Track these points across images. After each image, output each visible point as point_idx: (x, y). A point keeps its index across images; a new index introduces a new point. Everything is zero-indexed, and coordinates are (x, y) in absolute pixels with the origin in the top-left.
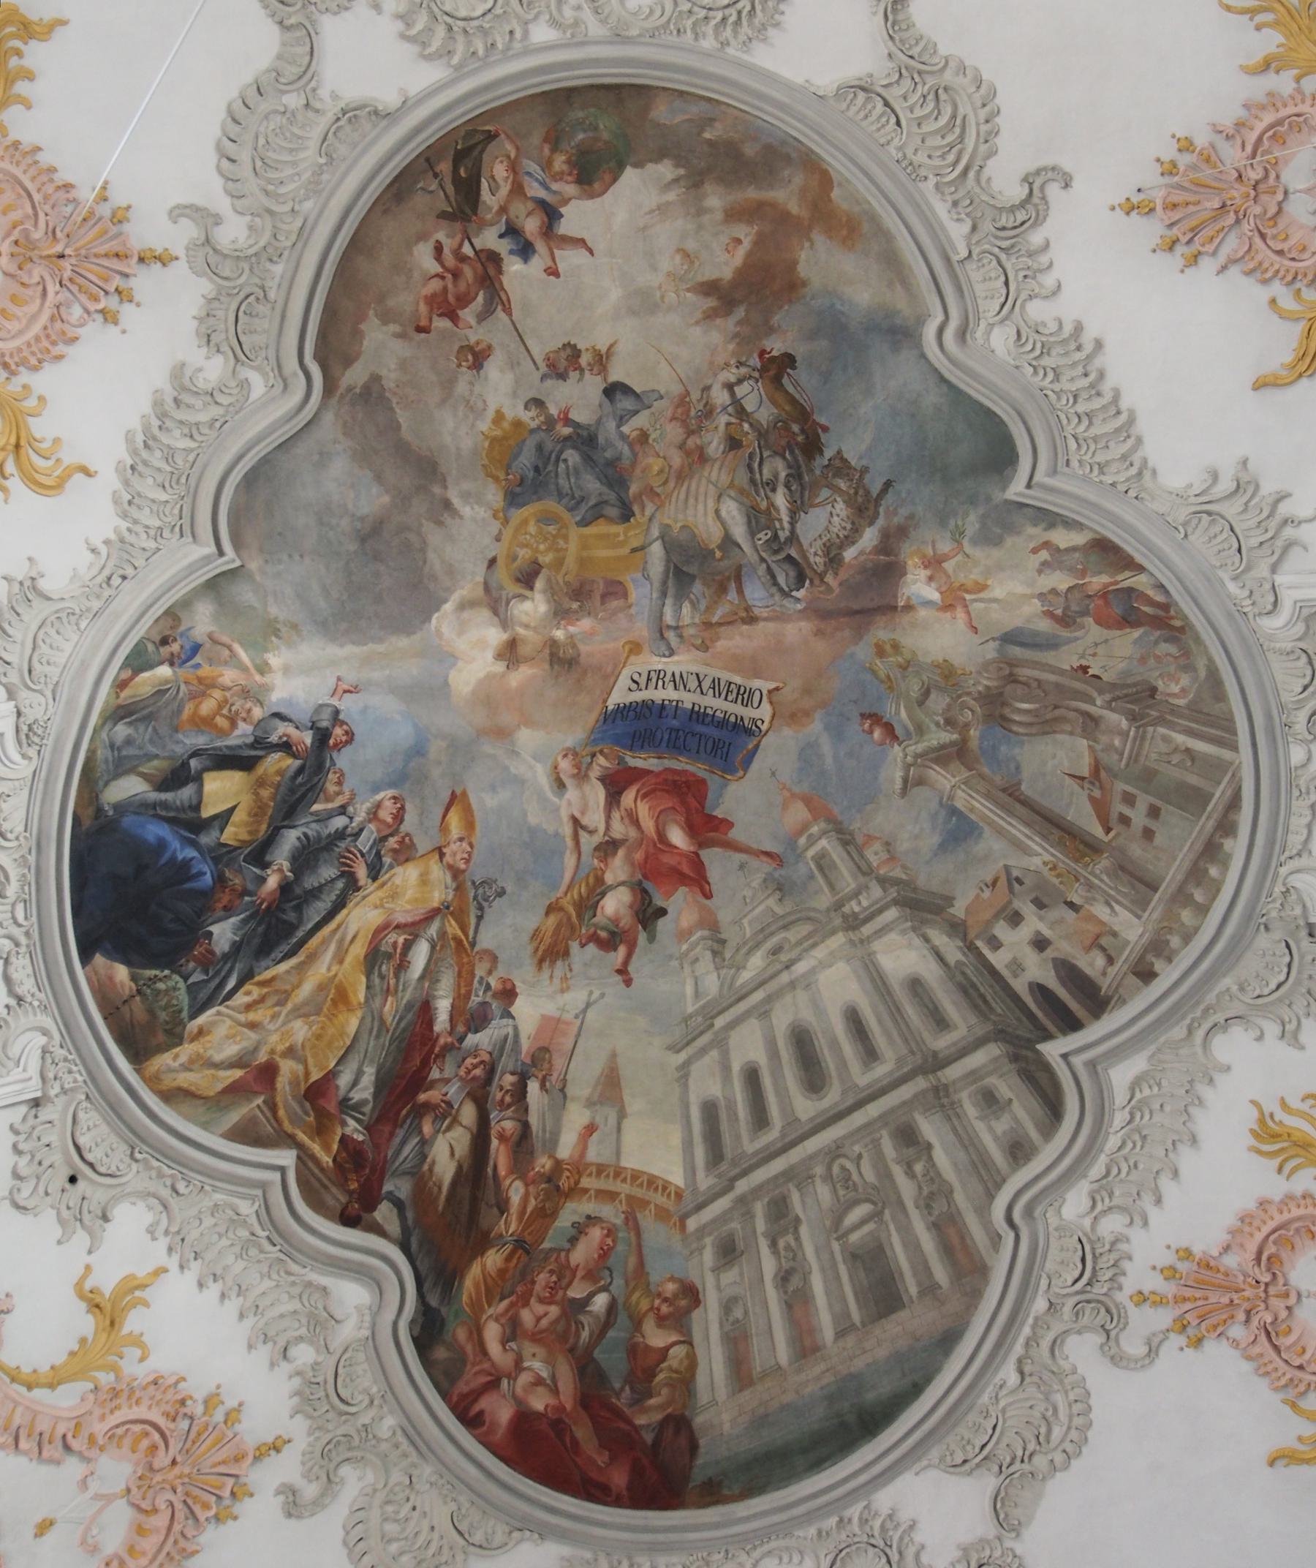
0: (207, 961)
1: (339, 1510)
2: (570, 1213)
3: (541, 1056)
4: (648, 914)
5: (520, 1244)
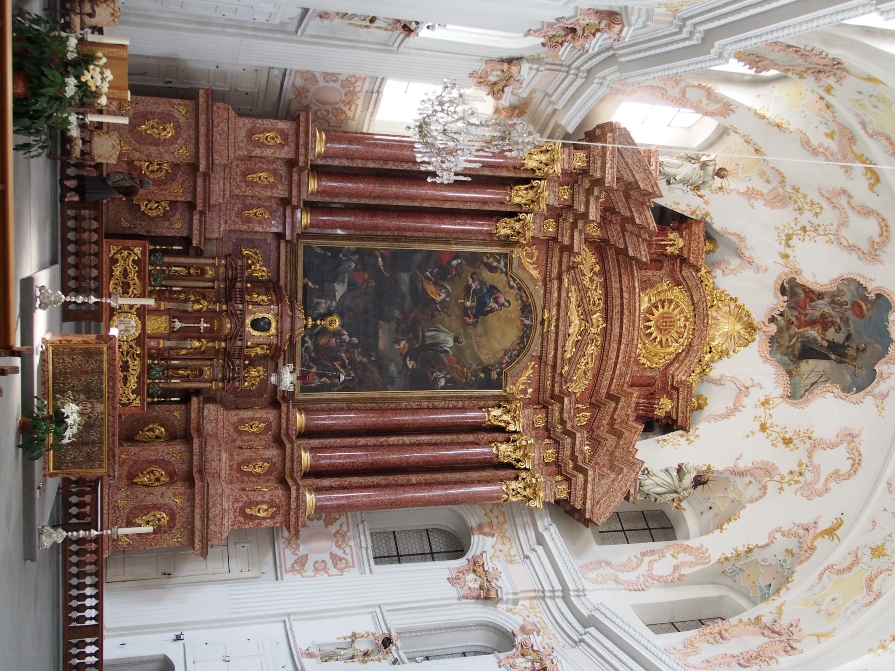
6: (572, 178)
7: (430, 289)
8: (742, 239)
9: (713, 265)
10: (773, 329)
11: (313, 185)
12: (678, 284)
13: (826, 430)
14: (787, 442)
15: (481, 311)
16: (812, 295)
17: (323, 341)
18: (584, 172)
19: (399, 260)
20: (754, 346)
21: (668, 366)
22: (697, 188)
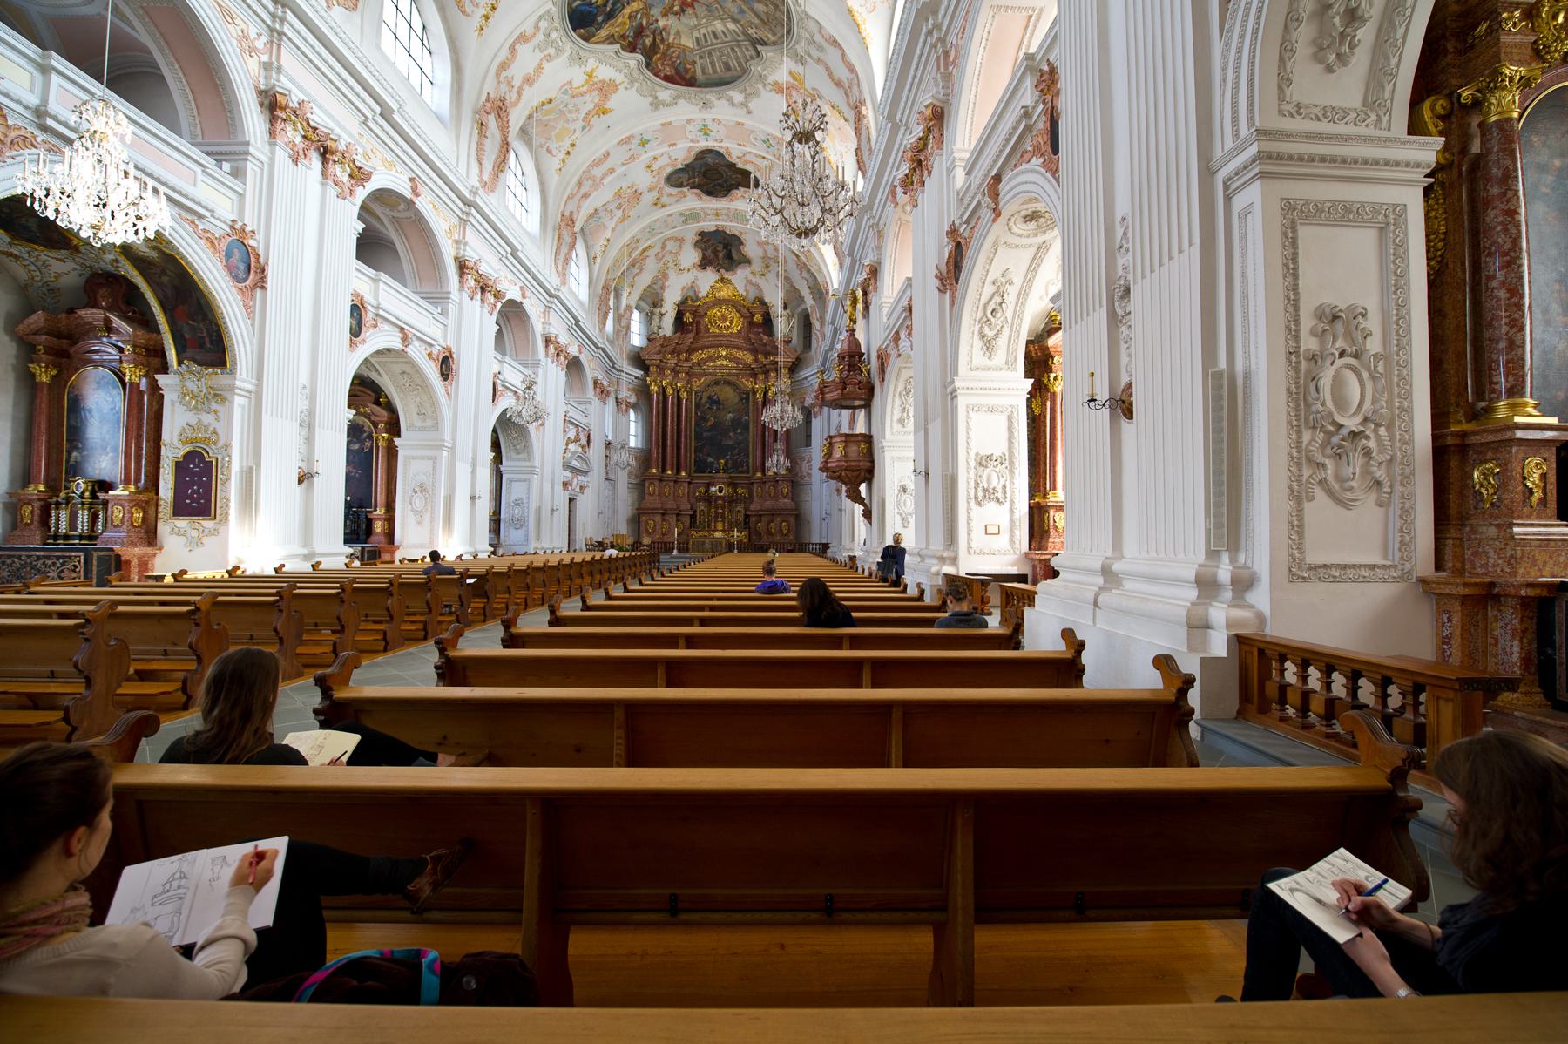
0: (598, 24)
1: (634, 89)
2: (672, 50)
3: (664, 29)
4: (683, 11)
5: (664, 54)
6: (661, 369)
7: (709, 424)
8: (684, 288)
9: (698, 299)
10: (722, 271)
11: (669, 472)
12: (706, 313)
13: (760, 252)
14: (767, 266)
15: (718, 402)
16: (704, 258)
17: (730, 466)
18: (658, 366)
19: (698, 437)
20: (730, 278)
21: (742, 316)
22: (662, 315)
